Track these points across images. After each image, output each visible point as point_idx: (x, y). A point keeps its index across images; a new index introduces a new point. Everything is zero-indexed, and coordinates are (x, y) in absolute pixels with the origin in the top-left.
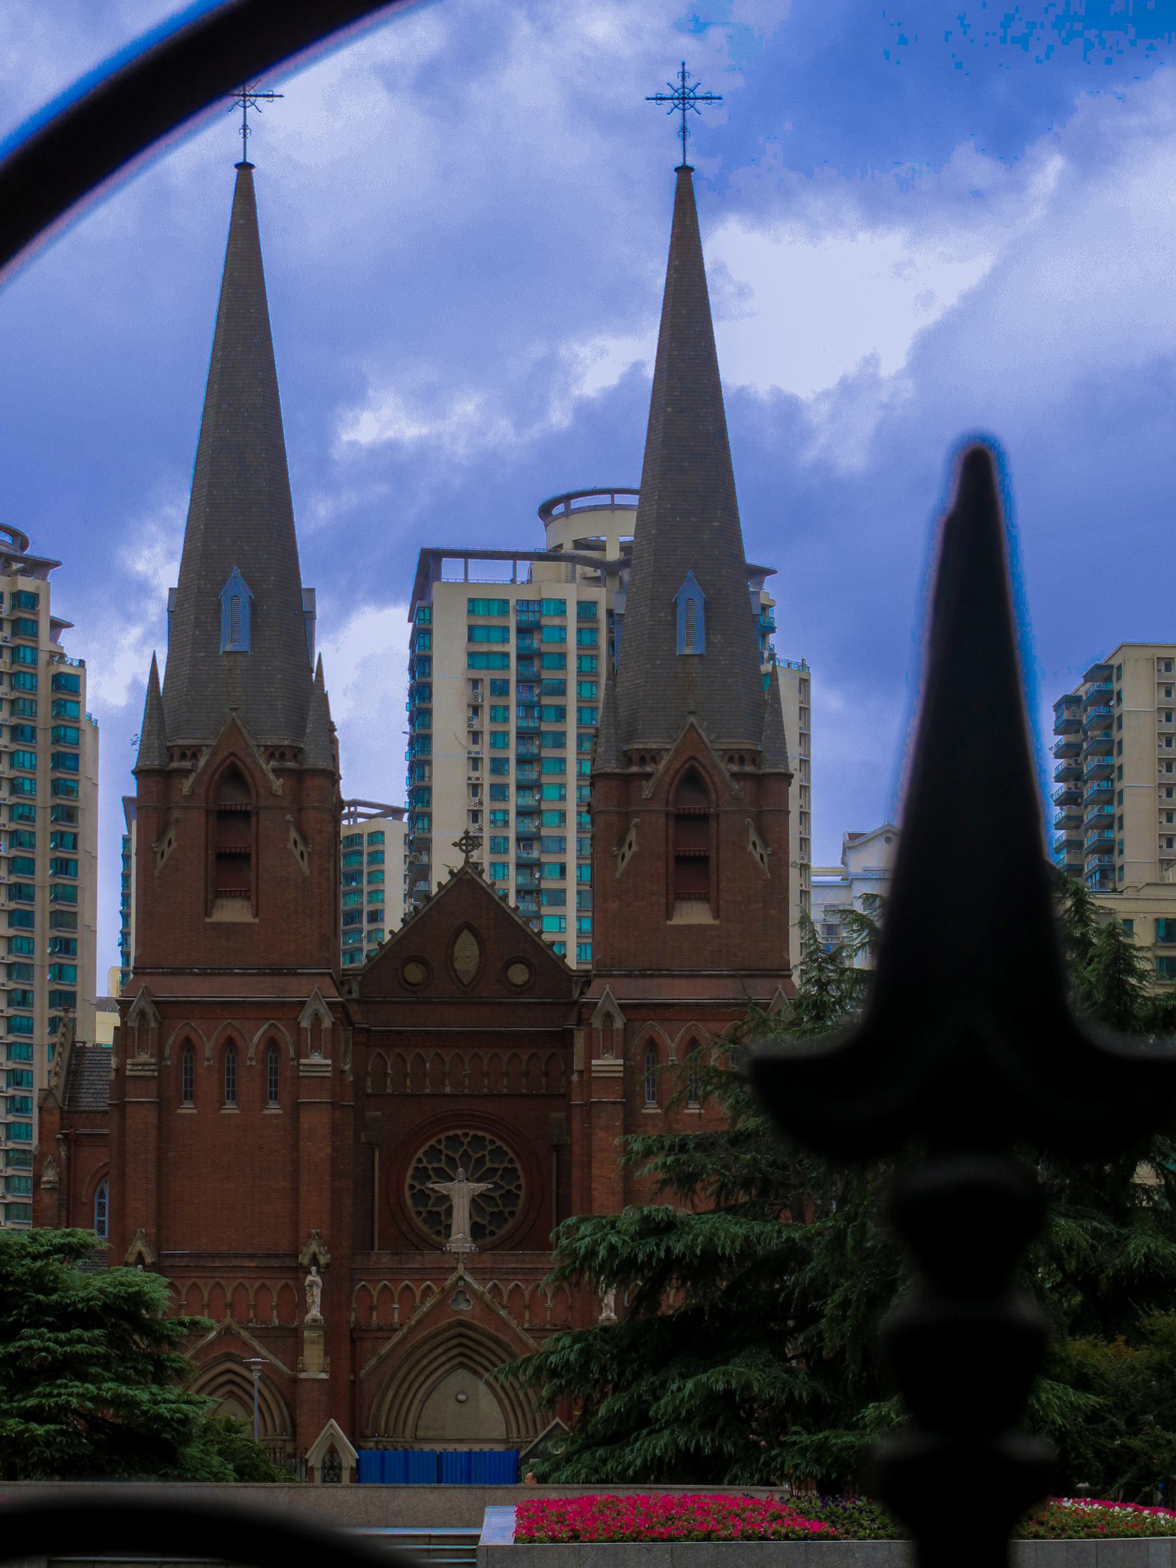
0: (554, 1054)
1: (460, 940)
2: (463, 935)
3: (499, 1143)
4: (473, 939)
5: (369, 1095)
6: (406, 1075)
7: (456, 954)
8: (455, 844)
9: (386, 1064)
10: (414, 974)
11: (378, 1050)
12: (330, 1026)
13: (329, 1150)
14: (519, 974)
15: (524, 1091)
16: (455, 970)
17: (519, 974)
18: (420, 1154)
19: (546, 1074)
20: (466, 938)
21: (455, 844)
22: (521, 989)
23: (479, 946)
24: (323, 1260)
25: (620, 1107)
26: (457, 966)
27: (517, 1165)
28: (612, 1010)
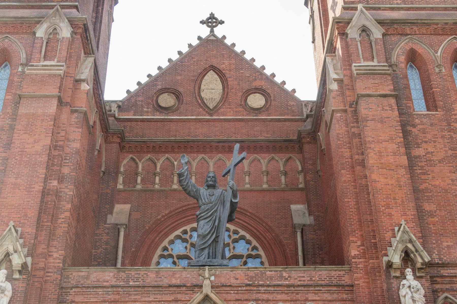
0: (290, 158)
1: (206, 77)
2: (209, 74)
3: (242, 233)
4: (216, 76)
5: (120, 191)
6: (155, 174)
7: (202, 87)
8: (202, 22)
9: (137, 167)
10: (167, 100)
11: (131, 156)
12: (69, 36)
13: (48, 142)
14: (256, 101)
15: (265, 186)
16: (202, 99)
17: (256, 101)
18: (165, 243)
19: (285, 174)
20: (211, 76)
21: (202, 22)
22: (258, 111)
23: (223, 83)
24: (17, 261)
25: (392, 101)
26: (203, 94)
27: (261, 252)
28: (368, 24)
